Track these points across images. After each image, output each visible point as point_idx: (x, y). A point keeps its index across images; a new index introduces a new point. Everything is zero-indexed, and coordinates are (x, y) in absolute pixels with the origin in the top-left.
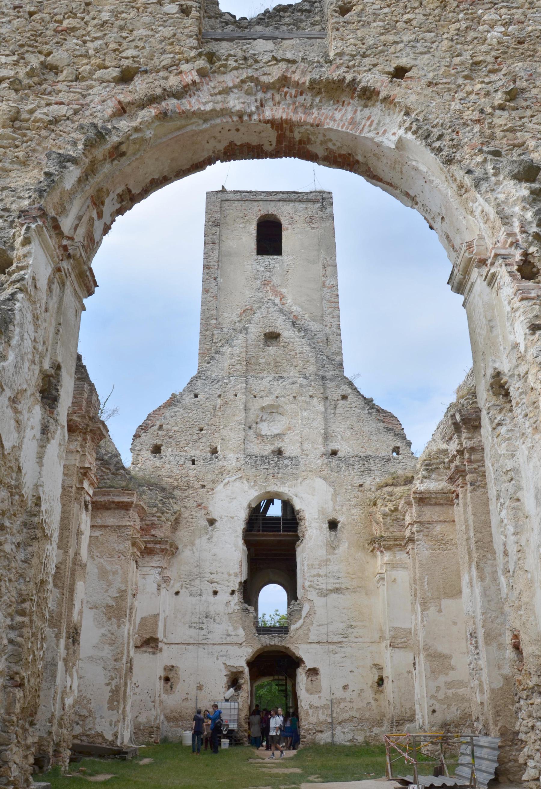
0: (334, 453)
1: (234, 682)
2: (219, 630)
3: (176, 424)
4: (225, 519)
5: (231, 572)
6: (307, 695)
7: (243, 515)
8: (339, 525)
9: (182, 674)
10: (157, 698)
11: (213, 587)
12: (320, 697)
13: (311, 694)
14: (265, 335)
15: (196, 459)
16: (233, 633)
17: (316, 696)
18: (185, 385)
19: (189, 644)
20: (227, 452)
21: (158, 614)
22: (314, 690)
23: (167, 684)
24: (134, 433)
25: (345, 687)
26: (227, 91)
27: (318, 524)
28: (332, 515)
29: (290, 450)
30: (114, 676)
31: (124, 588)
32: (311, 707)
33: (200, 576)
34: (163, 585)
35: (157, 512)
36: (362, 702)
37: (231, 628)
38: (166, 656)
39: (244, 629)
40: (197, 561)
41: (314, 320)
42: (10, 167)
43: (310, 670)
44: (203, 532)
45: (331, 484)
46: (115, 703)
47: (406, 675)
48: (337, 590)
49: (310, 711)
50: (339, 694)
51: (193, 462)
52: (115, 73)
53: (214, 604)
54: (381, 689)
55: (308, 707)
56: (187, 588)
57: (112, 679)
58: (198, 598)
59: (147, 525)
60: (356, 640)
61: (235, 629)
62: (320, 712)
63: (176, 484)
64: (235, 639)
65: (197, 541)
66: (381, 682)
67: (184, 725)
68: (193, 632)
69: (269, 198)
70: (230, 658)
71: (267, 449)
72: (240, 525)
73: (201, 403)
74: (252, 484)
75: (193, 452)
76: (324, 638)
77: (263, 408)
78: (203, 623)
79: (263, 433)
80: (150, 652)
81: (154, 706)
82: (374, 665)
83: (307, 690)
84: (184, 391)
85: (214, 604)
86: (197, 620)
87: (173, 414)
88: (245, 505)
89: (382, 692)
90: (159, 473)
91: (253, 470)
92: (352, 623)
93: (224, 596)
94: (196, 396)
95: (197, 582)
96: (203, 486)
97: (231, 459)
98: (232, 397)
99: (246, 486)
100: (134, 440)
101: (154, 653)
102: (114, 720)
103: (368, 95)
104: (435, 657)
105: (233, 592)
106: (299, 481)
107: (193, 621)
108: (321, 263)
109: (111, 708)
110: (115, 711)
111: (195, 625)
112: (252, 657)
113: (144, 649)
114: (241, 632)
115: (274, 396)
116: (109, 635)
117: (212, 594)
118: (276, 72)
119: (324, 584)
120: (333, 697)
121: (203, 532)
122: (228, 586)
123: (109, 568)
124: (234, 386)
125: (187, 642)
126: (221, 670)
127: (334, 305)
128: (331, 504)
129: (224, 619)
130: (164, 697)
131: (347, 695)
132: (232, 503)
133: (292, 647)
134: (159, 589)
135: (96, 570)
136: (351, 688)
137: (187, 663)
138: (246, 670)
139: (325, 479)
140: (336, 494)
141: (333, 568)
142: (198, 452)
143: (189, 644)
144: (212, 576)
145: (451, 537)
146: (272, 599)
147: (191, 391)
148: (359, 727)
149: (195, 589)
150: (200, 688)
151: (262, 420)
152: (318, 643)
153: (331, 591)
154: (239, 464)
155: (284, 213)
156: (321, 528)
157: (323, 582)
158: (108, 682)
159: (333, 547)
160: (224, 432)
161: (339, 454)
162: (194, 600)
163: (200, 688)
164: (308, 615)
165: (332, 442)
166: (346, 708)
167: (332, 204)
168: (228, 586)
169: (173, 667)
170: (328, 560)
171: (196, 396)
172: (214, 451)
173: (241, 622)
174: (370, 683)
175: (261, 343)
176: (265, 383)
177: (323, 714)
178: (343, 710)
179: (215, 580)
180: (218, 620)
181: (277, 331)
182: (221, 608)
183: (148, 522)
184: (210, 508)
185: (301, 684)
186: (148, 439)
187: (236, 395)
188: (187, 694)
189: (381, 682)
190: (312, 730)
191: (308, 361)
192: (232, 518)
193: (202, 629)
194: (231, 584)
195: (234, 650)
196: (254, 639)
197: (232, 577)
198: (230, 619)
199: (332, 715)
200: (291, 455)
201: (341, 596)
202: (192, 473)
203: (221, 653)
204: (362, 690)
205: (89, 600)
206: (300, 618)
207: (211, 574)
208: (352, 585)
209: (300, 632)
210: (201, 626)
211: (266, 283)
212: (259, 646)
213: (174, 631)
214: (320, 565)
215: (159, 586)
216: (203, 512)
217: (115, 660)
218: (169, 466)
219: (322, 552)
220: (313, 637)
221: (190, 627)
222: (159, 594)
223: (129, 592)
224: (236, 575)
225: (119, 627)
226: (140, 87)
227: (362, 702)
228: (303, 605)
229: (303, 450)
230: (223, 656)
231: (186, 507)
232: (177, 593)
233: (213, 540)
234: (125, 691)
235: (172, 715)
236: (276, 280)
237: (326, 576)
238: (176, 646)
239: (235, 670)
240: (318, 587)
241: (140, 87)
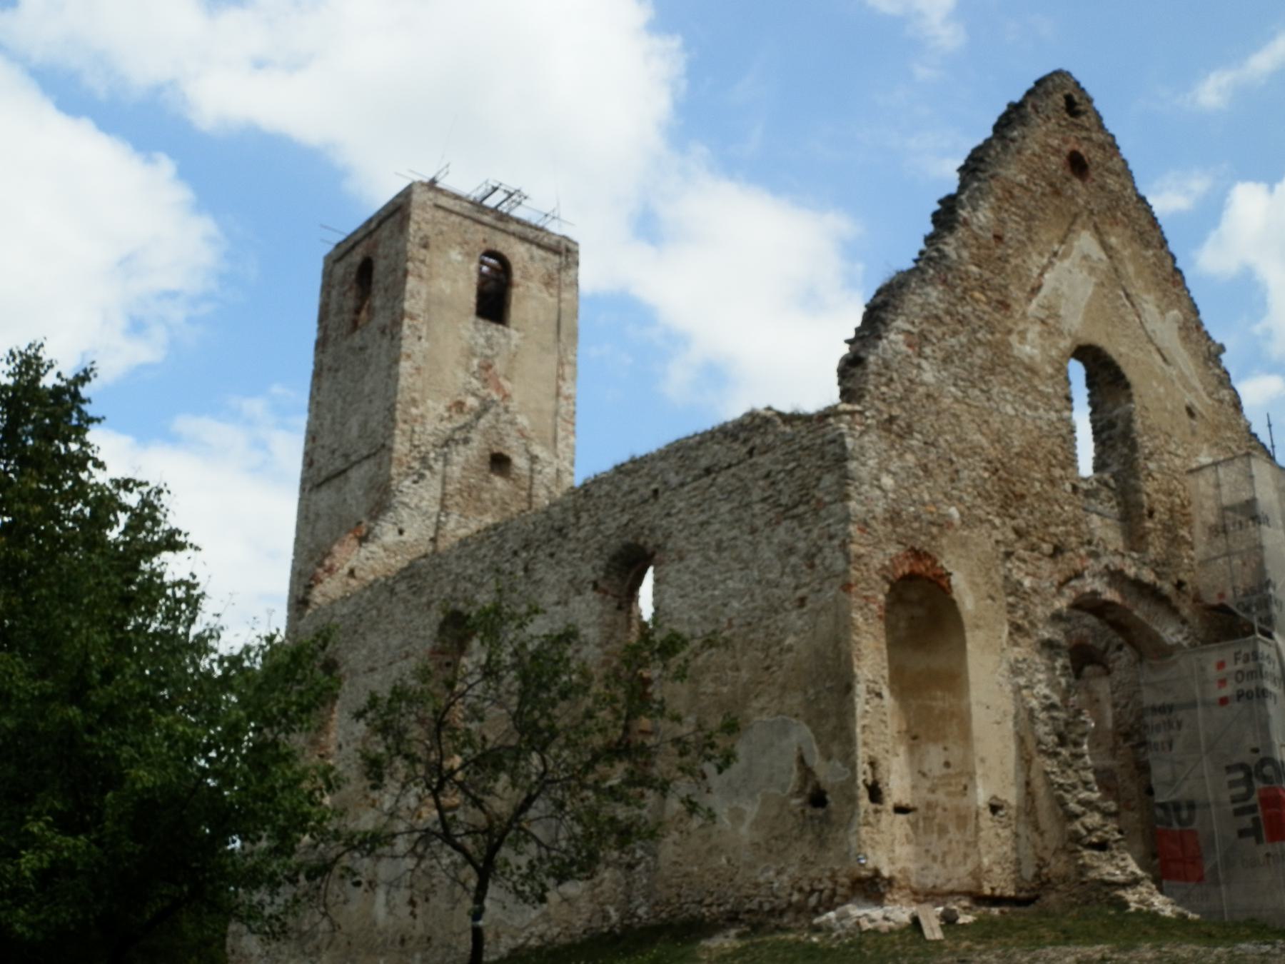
41: (544, 444)
94: (401, 532)
127: (570, 427)
155: (518, 253)
171: (401, 532)
175: (486, 467)
181: (506, 453)
211: (487, 367)
236: (499, 366)
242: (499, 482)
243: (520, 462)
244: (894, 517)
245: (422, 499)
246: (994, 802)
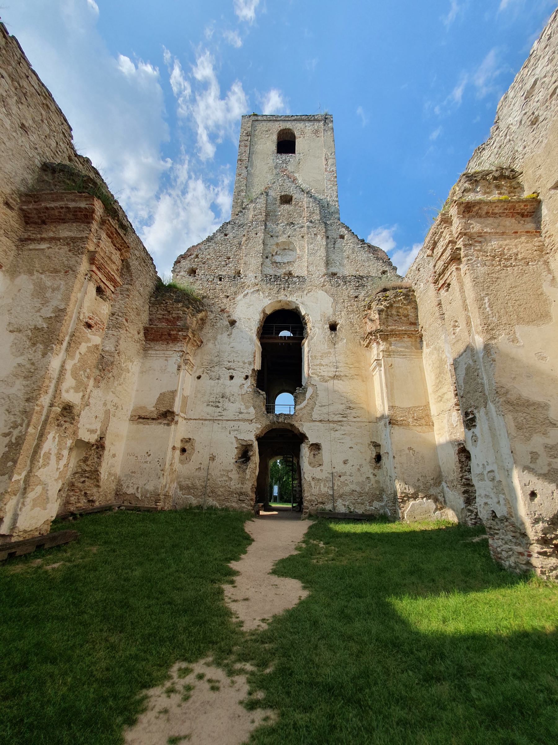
0: (334, 274)
3: (209, 254)
5: (246, 361)
6: (310, 468)
8: (338, 327)
9: (197, 445)
10: (167, 466)
11: (229, 373)
12: (321, 470)
13: (313, 467)
14: (281, 197)
15: (223, 277)
16: (245, 411)
19: (206, 420)
20: (247, 272)
23: (183, 454)
24: (175, 260)
25: (345, 462)
27: (321, 325)
28: (332, 319)
30: (19, 421)
31: (62, 307)
33: (219, 364)
35: (183, 306)
36: (361, 476)
37: (243, 407)
39: (255, 408)
40: (218, 352)
43: (312, 445)
44: (224, 329)
45: (332, 295)
46: (10, 464)
47: (407, 451)
49: (313, 483)
50: (340, 468)
53: (230, 386)
54: (378, 465)
55: (311, 479)
56: (208, 373)
57: (15, 426)
58: (217, 381)
59: (174, 318)
60: (355, 420)
61: (247, 407)
62: (322, 485)
64: (246, 416)
65: (219, 337)
66: (378, 458)
67: (195, 494)
68: (210, 409)
69: (287, 119)
70: (241, 433)
74: (267, 294)
76: (326, 417)
78: (219, 402)
80: (164, 424)
81: (163, 475)
82: (371, 442)
83: (310, 464)
84: (217, 231)
85: (230, 386)
88: (260, 309)
89: (379, 468)
90: (192, 287)
92: (351, 405)
93: (239, 380)
95: (217, 368)
97: (251, 275)
98: (254, 235)
100: (175, 265)
101: (168, 425)
104: (518, 405)
105: (247, 377)
106: (305, 293)
107: (210, 400)
108: (323, 158)
110: (7, 476)
111: (212, 404)
112: (262, 432)
113: (159, 421)
114: (252, 410)
116: (28, 366)
120: (334, 471)
121: (224, 329)
122: (242, 372)
123: (49, 284)
124: (256, 227)
125: (204, 418)
126: (232, 443)
128: (331, 311)
129: (238, 399)
131: (347, 469)
132: (250, 309)
133: (296, 425)
134: (179, 370)
135: (32, 287)
137: (203, 436)
138: (256, 444)
140: (336, 302)
142: (224, 273)
143: (206, 420)
145: (515, 251)
146: (284, 402)
147: (222, 232)
148: (358, 500)
149: (215, 374)
150: (213, 458)
157: (324, 370)
158: (7, 431)
163: (213, 458)
164: (311, 398)
165: (332, 267)
166: (346, 482)
167: (332, 121)
168: (242, 372)
169: (190, 439)
173: (252, 401)
174: (368, 459)
177: (325, 486)
178: (344, 484)
179: (232, 367)
180: (232, 399)
183: (174, 315)
185: (304, 458)
186: (186, 264)
187: (257, 234)
188: (201, 464)
189: (378, 458)
190: (314, 501)
192: (249, 319)
193: (218, 407)
194: (246, 370)
195: (245, 426)
196: (264, 416)
197: (247, 365)
198: (243, 399)
199: (333, 487)
201: (341, 382)
203: (233, 428)
205: (13, 321)
206: (304, 400)
207: (229, 362)
208: (350, 373)
209: (305, 411)
210: (217, 404)
215: (179, 367)
216: (225, 315)
217: (28, 400)
220: (315, 416)
221: (208, 405)
224: (250, 364)
225: (44, 355)
227: (361, 476)
228: (307, 388)
230: (235, 430)
231: (212, 312)
232: (199, 377)
233: (232, 336)
234: (38, 447)
237: (326, 365)
238: (194, 421)
239: (245, 443)
240: (320, 374)
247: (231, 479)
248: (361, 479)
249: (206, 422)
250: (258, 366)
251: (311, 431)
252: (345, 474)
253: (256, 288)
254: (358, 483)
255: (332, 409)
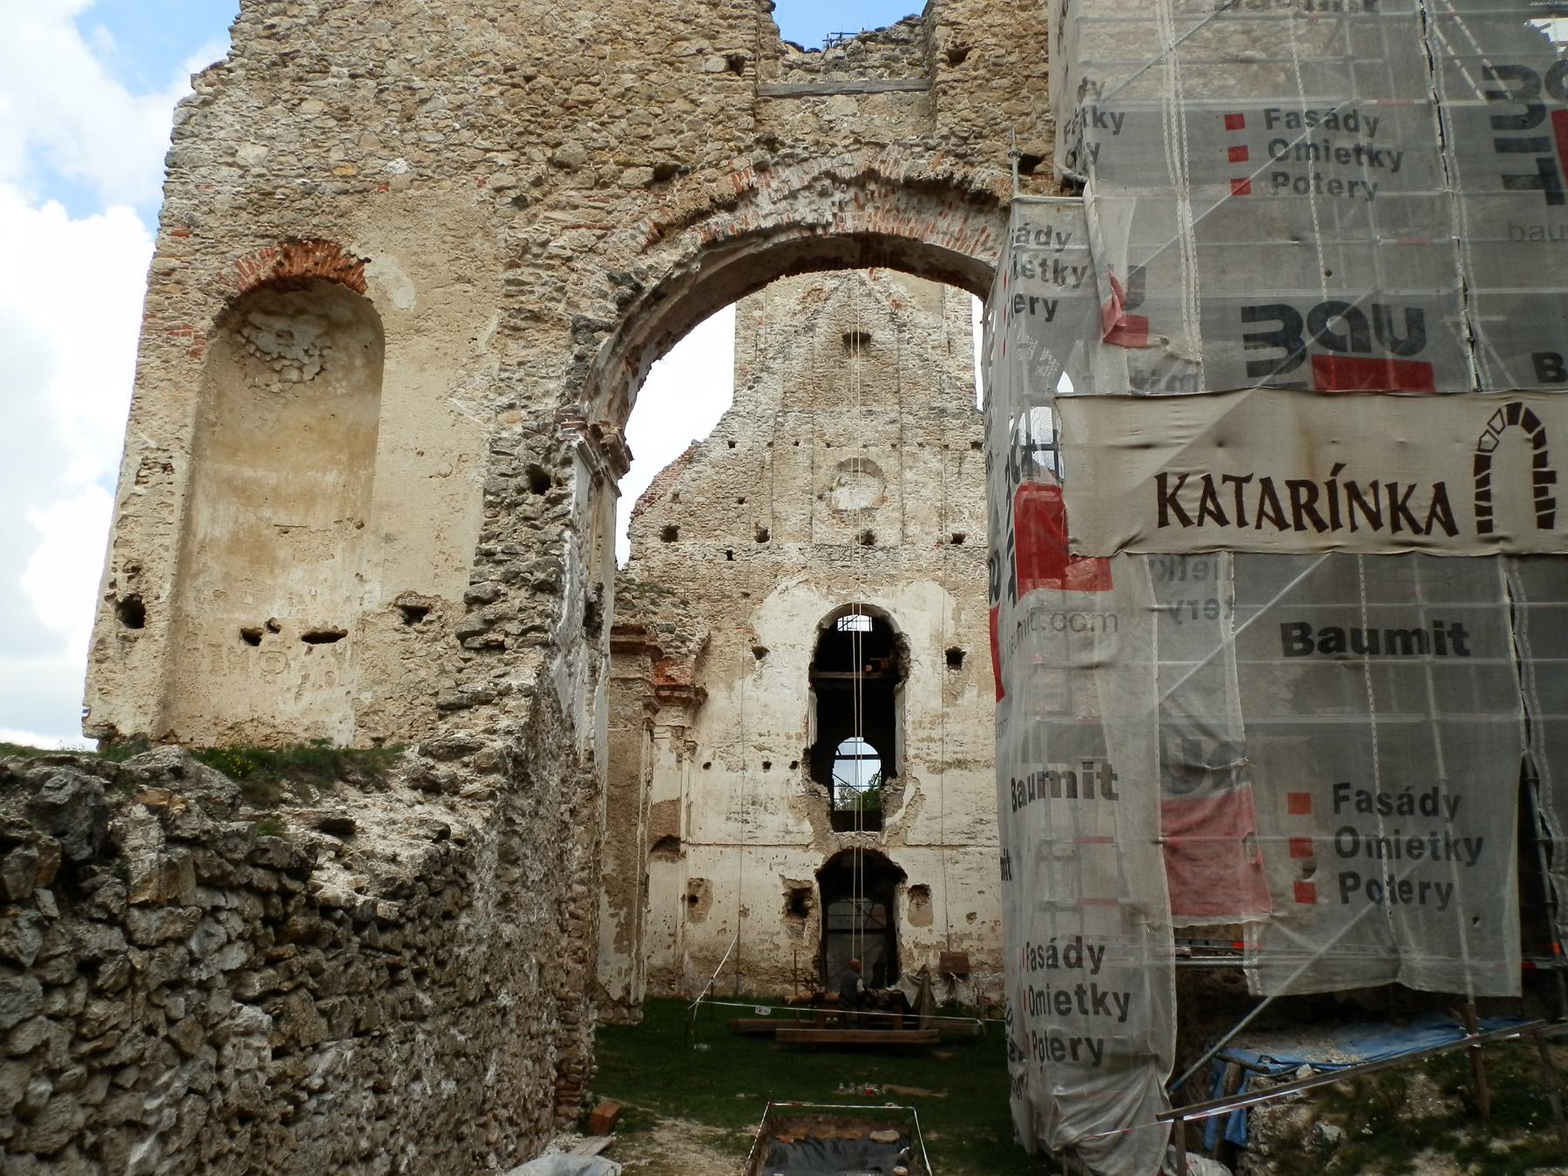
0: (958, 539)
1: (797, 902)
2: (773, 824)
4: (781, 649)
5: (792, 733)
6: (910, 927)
7: (810, 640)
9: (716, 893)
16: (795, 829)
17: (925, 929)
18: (714, 426)
21: (679, 800)
22: (919, 920)
25: (971, 917)
26: (793, 195)
28: (952, 642)
29: (887, 535)
32: (916, 945)
33: (742, 738)
34: (687, 755)
37: (791, 822)
38: (695, 864)
41: (928, 309)
42: (523, 324)
43: (915, 887)
45: (953, 589)
48: (960, 764)
49: (916, 953)
50: (961, 926)
51: (730, 555)
52: (647, 174)
60: (989, 843)
61: (799, 821)
63: (702, 591)
64: (799, 839)
65: (738, 683)
68: (733, 827)
71: (852, 532)
72: (806, 659)
73: (741, 456)
75: (728, 540)
76: (935, 839)
77: (842, 466)
79: (841, 507)
83: (911, 920)
86: (738, 809)
87: (695, 476)
88: (814, 625)
91: (825, 568)
92: (984, 817)
93: (780, 771)
94: (732, 445)
95: (738, 749)
96: (746, 595)
97: (791, 551)
98: (791, 447)
99: (814, 596)
101: (673, 861)
102: (625, 966)
103: (983, 202)
105: (794, 765)
109: (619, 950)
114: (807, 826)
115: (861, 443)
117: (761, 767)
118: (858, 162)
119: (937, 753)
120: (951, 931)
128: (950, 626)
130: (689, 925)
131: (974, 928)
132: (791, 623)
136: (979, 918)
138: (816, 886)
139: (942, 584)
140: (958, 610)
141: (953, 727)
142: (736, 540)
144: (762, 740)
150: (744, 913)
151: (840, 485)
152: (929, 845)
153: (950, 764)
154: (802, 560)
156: (934, 664)
159: (951, 695)
160: (778, 507)
161: (967, 542)
162: (733, 776)
163: (744, 913)
170: (943, 716)
171: (732, 445)
172: (763, 537)
176: (845, 420)
180: (771, 808)
182: (775, 790)
184: (759, 631)
186: (658, 518)
187: (797, 444)
191: (915, 384)
192: (793, 646)
195: (795, 855)
197: (794, 741)
200: (888, 545)
201: (966, 772)
202: (727, 573)
204: (996, 922)
212: (835, 849)
213: (706, 825)
214: (932, 723)
215: (680, 756)
218: (690, 563)
219: (936, 703)
221: (728, 819)
222: (680, 769)
223: (643, 779)
224: (799, 737)
226: (679, 197)
229: (905, 536)
231: (719, 630)
232: (707, 766)
235: (701, 955)
241: (679, 197)
242: (857, 363)
243: (882, 335)
244: (261, 199)
245: (758, 404)
246: (411, 602)
247: (777, 947)
248: (994, 945)
249: (728, 850)
250: (811, 741)
251: (914, 865)
252: (969, 936)
253: (803, 576)
254: (991, 951)
255: (948, 823)
